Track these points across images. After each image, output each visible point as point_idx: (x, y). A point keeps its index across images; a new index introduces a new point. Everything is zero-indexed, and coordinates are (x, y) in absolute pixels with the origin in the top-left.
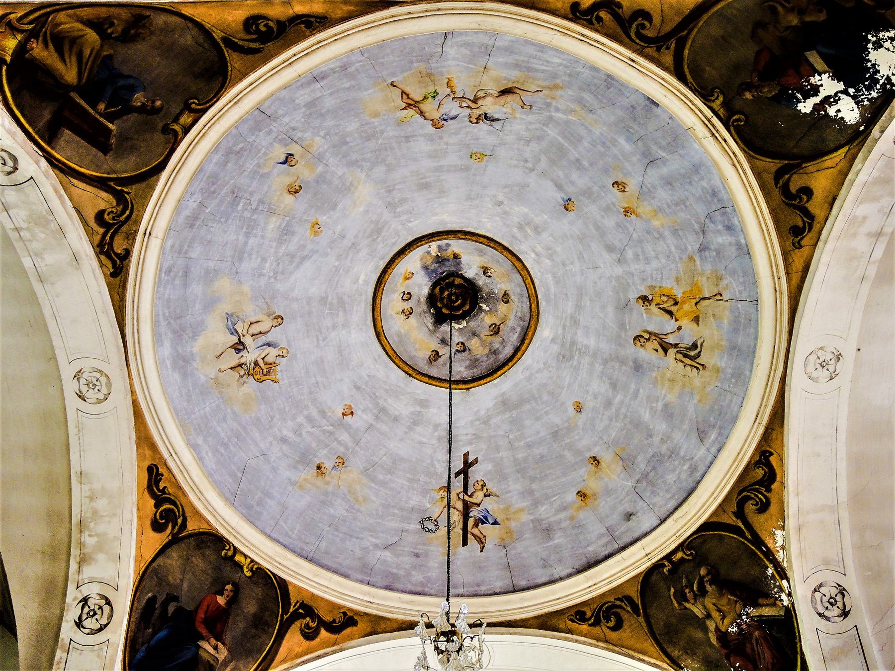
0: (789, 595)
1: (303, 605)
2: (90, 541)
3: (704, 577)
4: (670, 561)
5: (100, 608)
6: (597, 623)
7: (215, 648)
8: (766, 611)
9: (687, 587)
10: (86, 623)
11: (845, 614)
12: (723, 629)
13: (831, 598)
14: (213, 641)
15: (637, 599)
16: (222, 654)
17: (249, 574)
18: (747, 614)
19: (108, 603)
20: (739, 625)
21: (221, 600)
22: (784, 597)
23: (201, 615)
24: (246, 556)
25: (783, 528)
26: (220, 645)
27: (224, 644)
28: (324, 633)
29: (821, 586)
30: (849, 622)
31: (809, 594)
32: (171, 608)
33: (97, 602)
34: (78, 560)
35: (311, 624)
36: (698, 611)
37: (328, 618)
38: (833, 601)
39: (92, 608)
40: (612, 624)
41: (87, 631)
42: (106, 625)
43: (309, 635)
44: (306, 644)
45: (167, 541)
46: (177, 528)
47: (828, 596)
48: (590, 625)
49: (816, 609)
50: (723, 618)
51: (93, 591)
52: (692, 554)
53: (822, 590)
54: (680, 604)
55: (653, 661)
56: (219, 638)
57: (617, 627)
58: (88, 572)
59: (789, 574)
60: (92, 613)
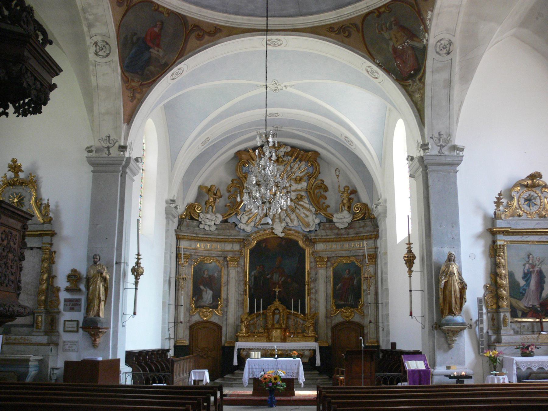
0: (427, 40)
1: (195, 26)
2: (91, 17)
3: (392, 22)
4: (379, 12)
5: (104, 46)
6: (339, 33)
7: (158, 51)
8: (415, 44)
9: (384, 24)
10: (100, 53)
11: (448, 53)
12: (396, 46)
13: (444, 45)
14: (156, 48)
15: (360, 25)
16: (161, 53)
17: (167, 15)
18: (408, 42)
19: (107, 44)
20: (403, 46)
21: (156, 30)
22: (425, 40)
23: (148, 38)
24: (164, 8)
25: (432, 11)
26: (160, 50)
27: (162, 49)
28: (207, 37)
29: (441, 40)
30: (449, 57)
31: (435, 43)
32: (135, 39)
33: (102, 44)
34: (87, 25)
35: (200, 34)
36: (386, 35)
37: (208, 30)
38: (445, 47)
39: (100, 46)
40: (347, 34)
41: (101, 57)
42: (109, 54)
43: (200, 38)
44: (198, 42)
45: (126, 9)
46: (129, 2)
47: (443, 45)
48: (336, 34)
49: (436, 50)
50: (397, 41)
51: (98, 39)
52: (389, 10)
53: (442, 42)
54: (379, 31)
55: (362, 54)
56: (158, 46)
57: (349, 36)
58: (94, 31)
59: (429, 32)
60: (101, 49)
